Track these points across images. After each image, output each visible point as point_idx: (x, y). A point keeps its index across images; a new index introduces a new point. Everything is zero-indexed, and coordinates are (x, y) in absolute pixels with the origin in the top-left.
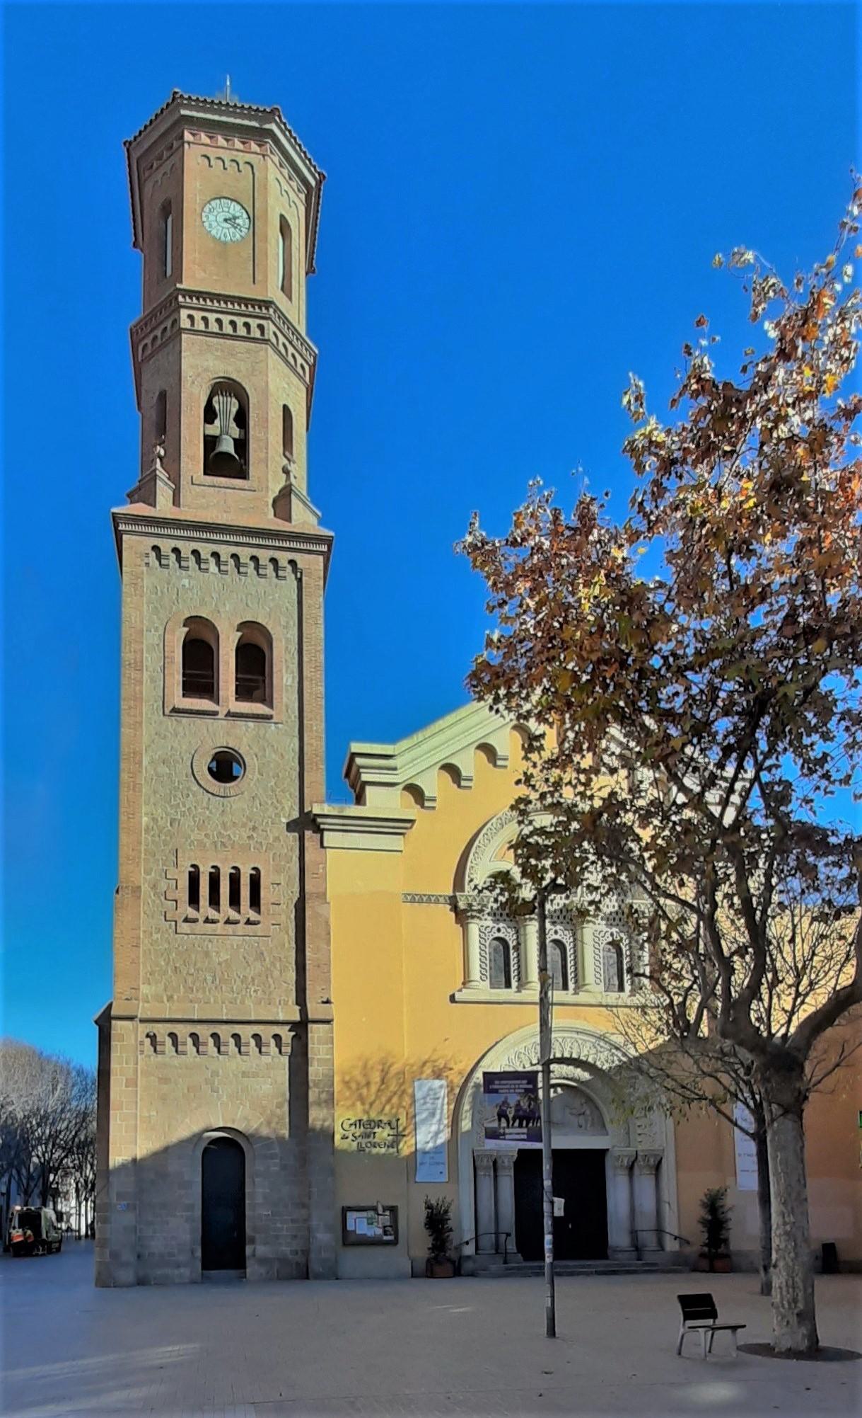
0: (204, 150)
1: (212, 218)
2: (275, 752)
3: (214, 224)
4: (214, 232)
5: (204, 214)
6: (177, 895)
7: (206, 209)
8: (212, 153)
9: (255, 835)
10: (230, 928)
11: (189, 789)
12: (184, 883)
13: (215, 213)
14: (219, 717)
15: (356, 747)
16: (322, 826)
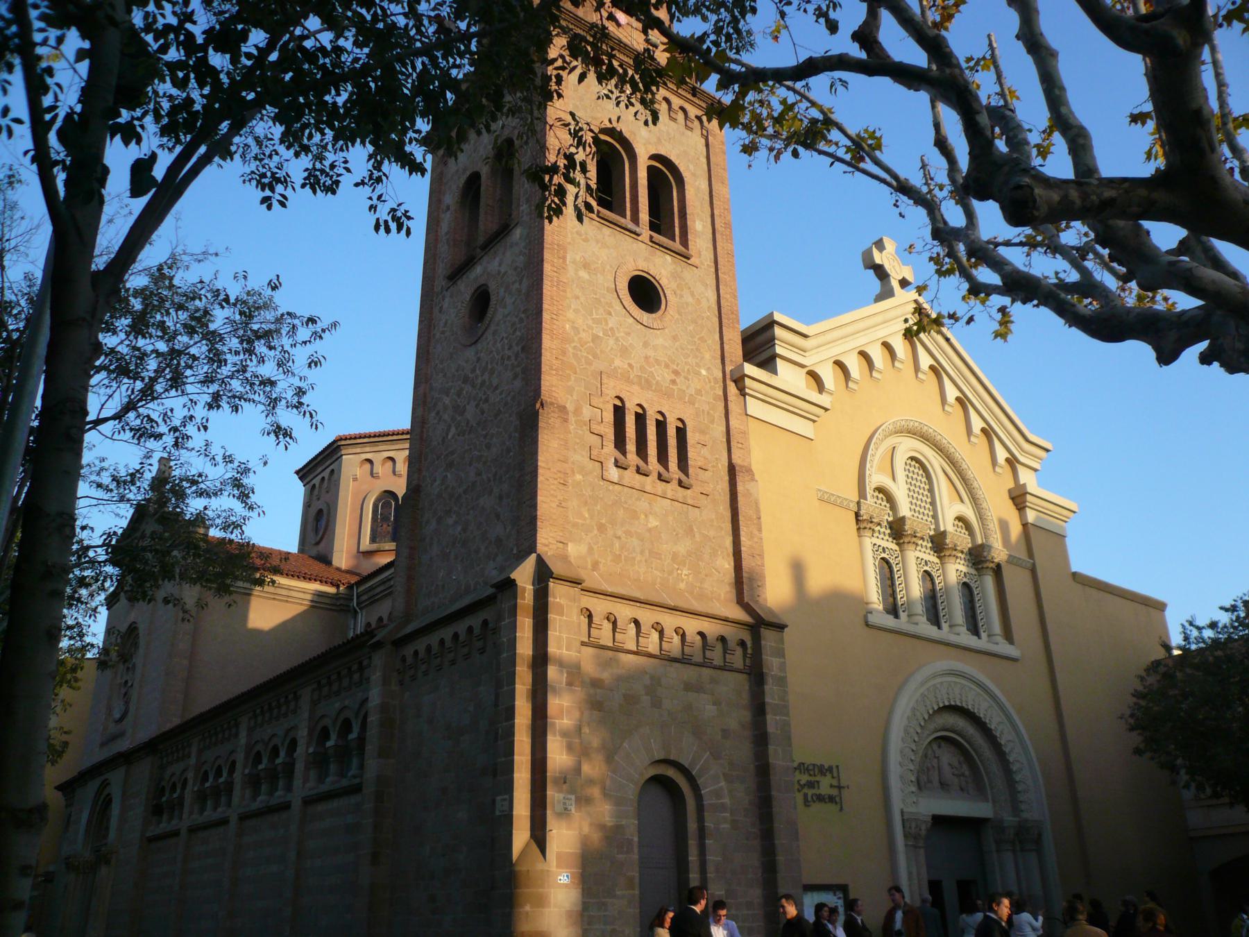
2: (692, 294)
9: (678, 381)
11: (610, 305)
12: (609, 416)
14: (639, 238)
15: (778, 317)
16: (747, 391)
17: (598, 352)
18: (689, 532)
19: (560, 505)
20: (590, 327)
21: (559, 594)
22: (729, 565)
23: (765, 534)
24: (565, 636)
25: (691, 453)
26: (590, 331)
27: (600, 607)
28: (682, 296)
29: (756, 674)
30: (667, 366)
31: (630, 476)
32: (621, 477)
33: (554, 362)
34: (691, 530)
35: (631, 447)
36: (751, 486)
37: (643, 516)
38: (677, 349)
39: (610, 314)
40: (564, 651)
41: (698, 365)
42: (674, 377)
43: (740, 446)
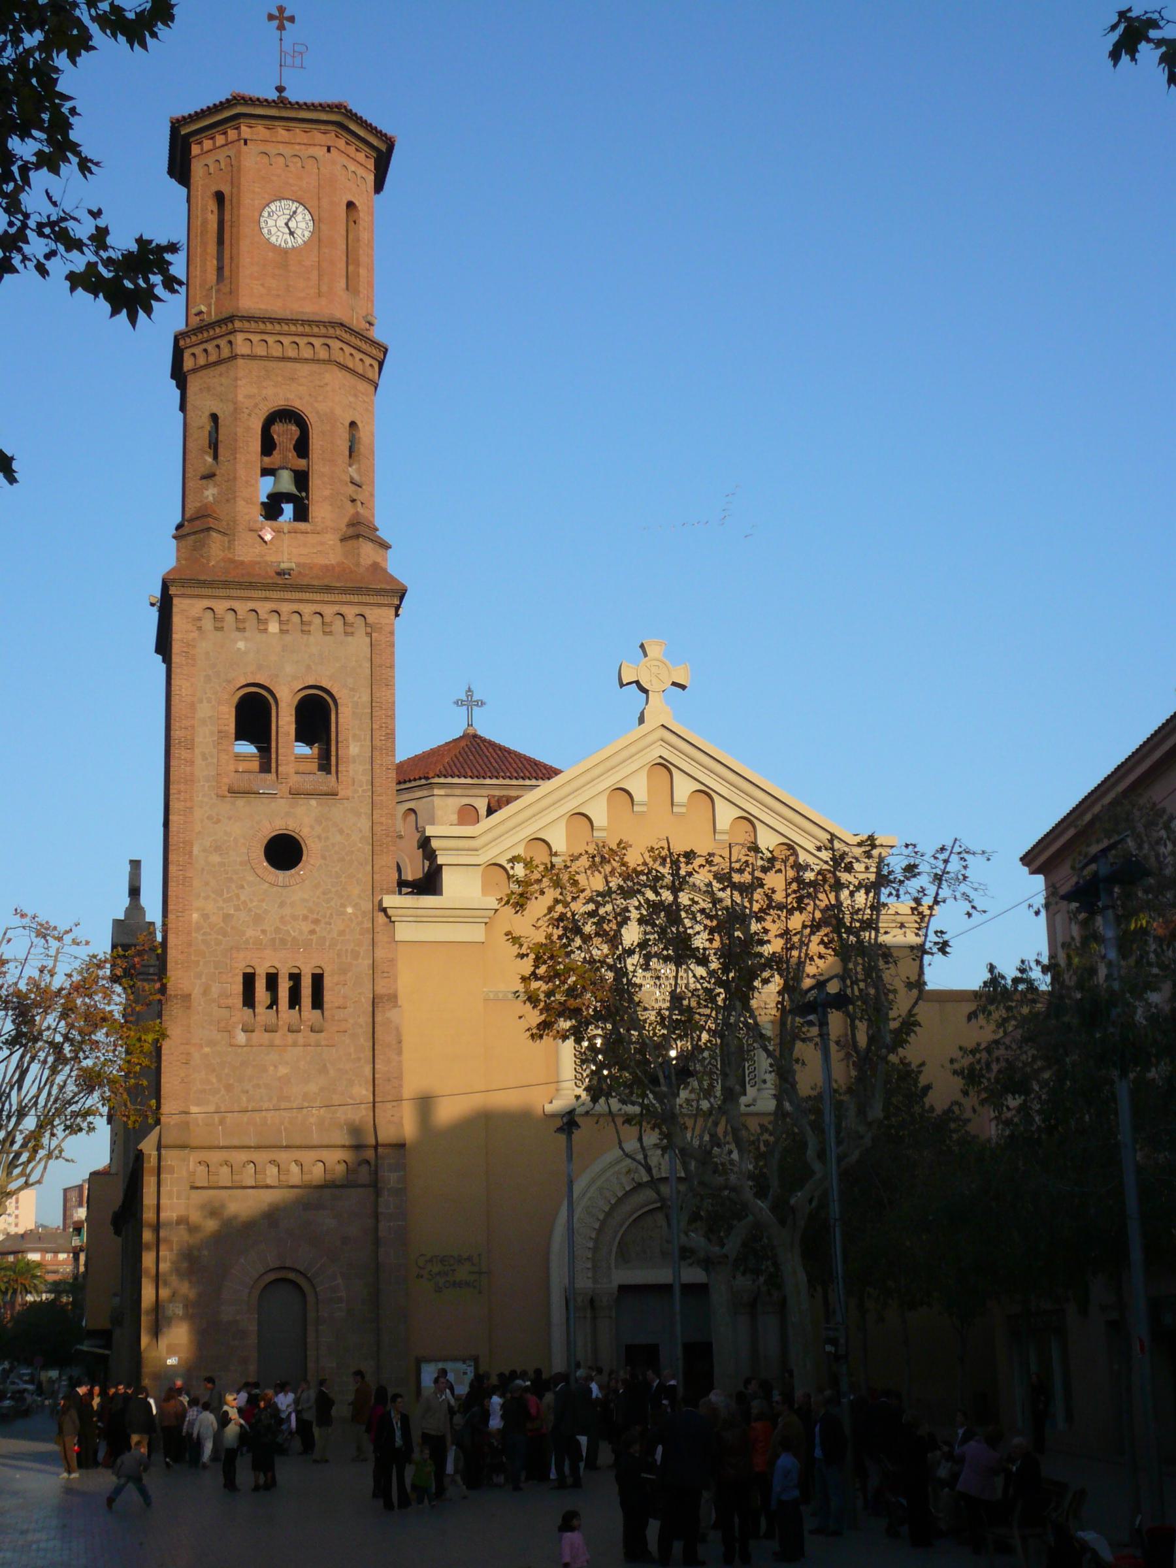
0: (263, 148)
1: (271, 223)
2: (341, 832)
3: (274, 230)
4: (273, 239)
5: (262, 219)
6: (230, 1001)
7: (265, 214)
8: (272, 149)
9: (318, 929)
10: (291, 1037)
12: (239, 988)
13: (275, 217)
16: (393, 919)
17: (229, 929)
18: (323, 1070)
19: (182, 1081)
20: (222, 909)
21: (171, 1158)
22: (367, 1090)
23: (407, 1055)
24: (175, 1189)
25: (328, 997)
26: (221, 912)
27: (215, 1157)
28: (327, 838)
29: (375, 1185)
30: (305, 918)
31: (259, 1036)
32: (248, 1040)
33: (179, 957)
34: (325, 1066)
35: (260, 1008)
36: (392, 1014)
37: (272, 1068)
38: (318, 897)
39: (242, 887)
40: (175, 1201)
41: (344, 906)
42: (313, 927)
43: (385, 975)
